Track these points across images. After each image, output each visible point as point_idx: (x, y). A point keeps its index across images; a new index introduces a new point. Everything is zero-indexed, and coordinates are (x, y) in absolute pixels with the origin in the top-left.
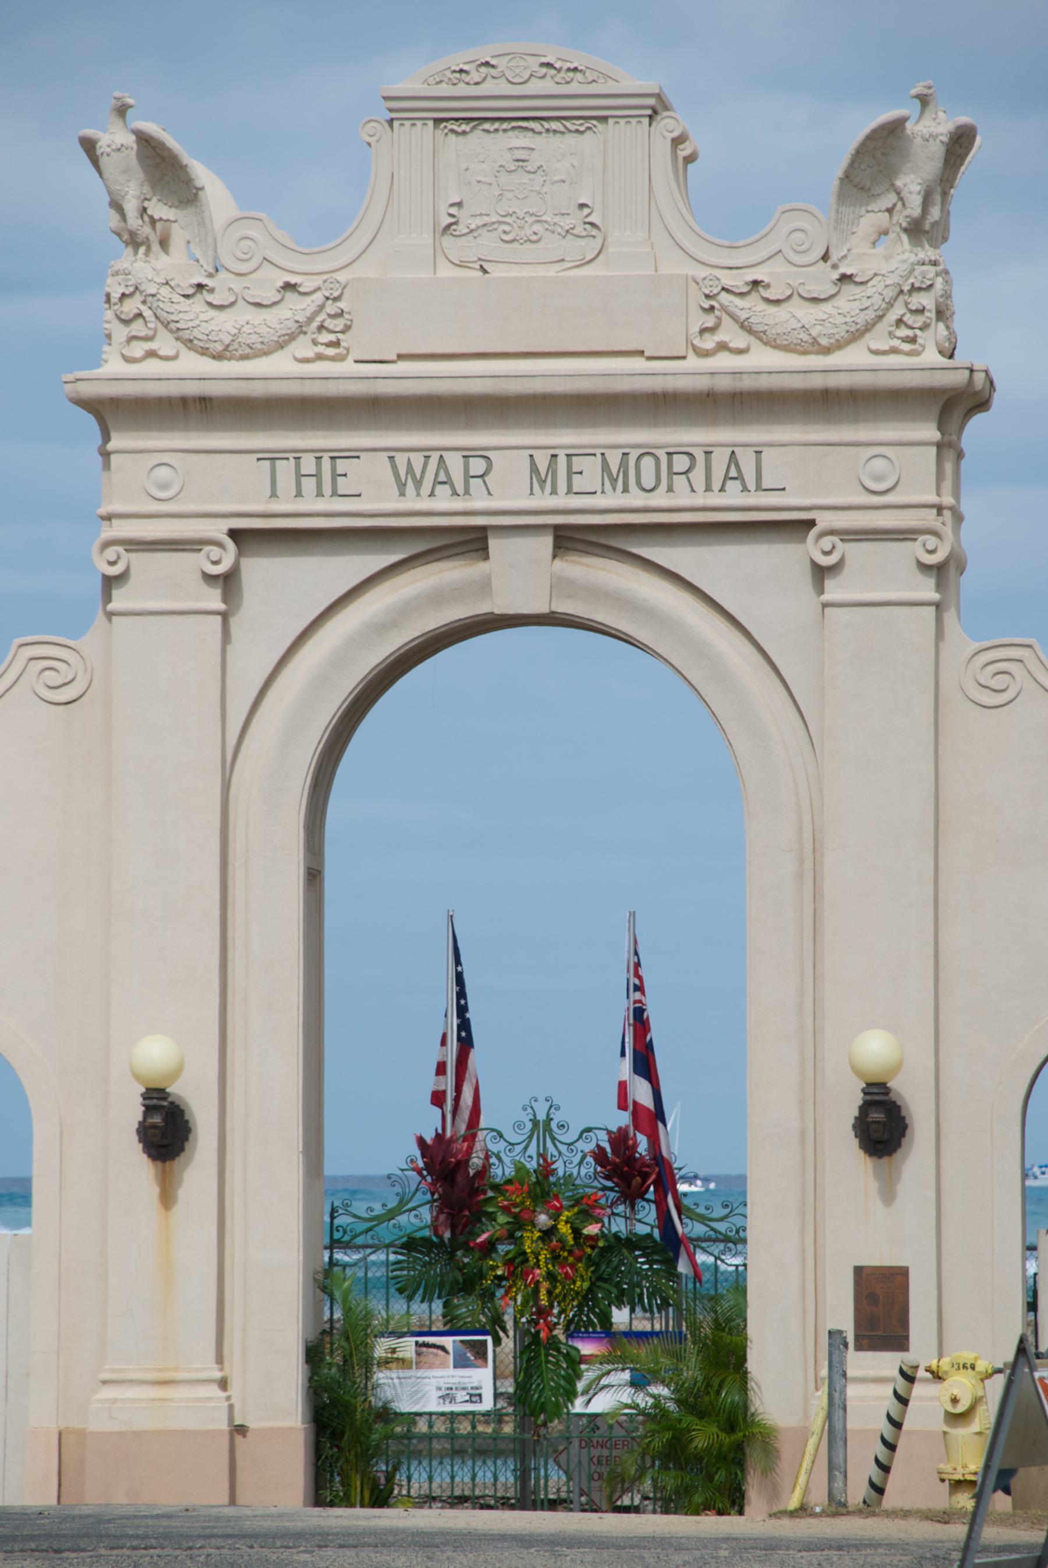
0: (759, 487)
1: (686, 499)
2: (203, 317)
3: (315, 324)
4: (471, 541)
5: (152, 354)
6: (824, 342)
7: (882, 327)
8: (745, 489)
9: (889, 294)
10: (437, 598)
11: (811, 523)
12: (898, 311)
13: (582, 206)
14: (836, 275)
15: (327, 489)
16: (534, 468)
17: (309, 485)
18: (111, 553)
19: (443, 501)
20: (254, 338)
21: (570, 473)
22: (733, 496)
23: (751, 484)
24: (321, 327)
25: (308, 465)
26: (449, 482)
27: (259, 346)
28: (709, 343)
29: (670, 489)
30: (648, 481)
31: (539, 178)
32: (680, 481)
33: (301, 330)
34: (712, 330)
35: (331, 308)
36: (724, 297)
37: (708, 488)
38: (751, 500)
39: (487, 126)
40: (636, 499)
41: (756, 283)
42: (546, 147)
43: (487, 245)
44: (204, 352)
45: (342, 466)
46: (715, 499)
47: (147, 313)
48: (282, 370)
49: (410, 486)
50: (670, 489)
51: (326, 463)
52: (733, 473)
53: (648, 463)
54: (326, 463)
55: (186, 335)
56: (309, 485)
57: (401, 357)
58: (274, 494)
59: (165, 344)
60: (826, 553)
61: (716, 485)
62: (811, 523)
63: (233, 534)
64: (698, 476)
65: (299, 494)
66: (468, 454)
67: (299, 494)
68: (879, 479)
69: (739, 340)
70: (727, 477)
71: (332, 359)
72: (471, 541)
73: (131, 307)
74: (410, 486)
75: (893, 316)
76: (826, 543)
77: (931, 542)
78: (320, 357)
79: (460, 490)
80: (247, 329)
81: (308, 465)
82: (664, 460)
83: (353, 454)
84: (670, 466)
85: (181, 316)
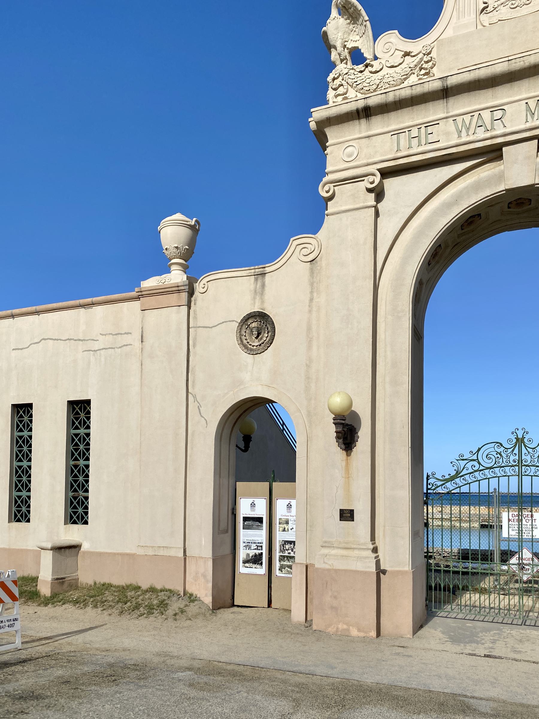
2: (367, 77)
3: (418, 69)
4: (493, 153)
15: (423, 142)
16: (528, 108)
17: (415, 142)
18: (326, 188)
19: (481, 134)
24: (421, 69)
27: (392, 83)
35: (425, 59)
45: (430, 130)
47: (343, 82)
51: (423, 130)
54: (423, 130)
55: (360, 87)
66: (493, 109)
80: (387, 76)
85: (358, 79)
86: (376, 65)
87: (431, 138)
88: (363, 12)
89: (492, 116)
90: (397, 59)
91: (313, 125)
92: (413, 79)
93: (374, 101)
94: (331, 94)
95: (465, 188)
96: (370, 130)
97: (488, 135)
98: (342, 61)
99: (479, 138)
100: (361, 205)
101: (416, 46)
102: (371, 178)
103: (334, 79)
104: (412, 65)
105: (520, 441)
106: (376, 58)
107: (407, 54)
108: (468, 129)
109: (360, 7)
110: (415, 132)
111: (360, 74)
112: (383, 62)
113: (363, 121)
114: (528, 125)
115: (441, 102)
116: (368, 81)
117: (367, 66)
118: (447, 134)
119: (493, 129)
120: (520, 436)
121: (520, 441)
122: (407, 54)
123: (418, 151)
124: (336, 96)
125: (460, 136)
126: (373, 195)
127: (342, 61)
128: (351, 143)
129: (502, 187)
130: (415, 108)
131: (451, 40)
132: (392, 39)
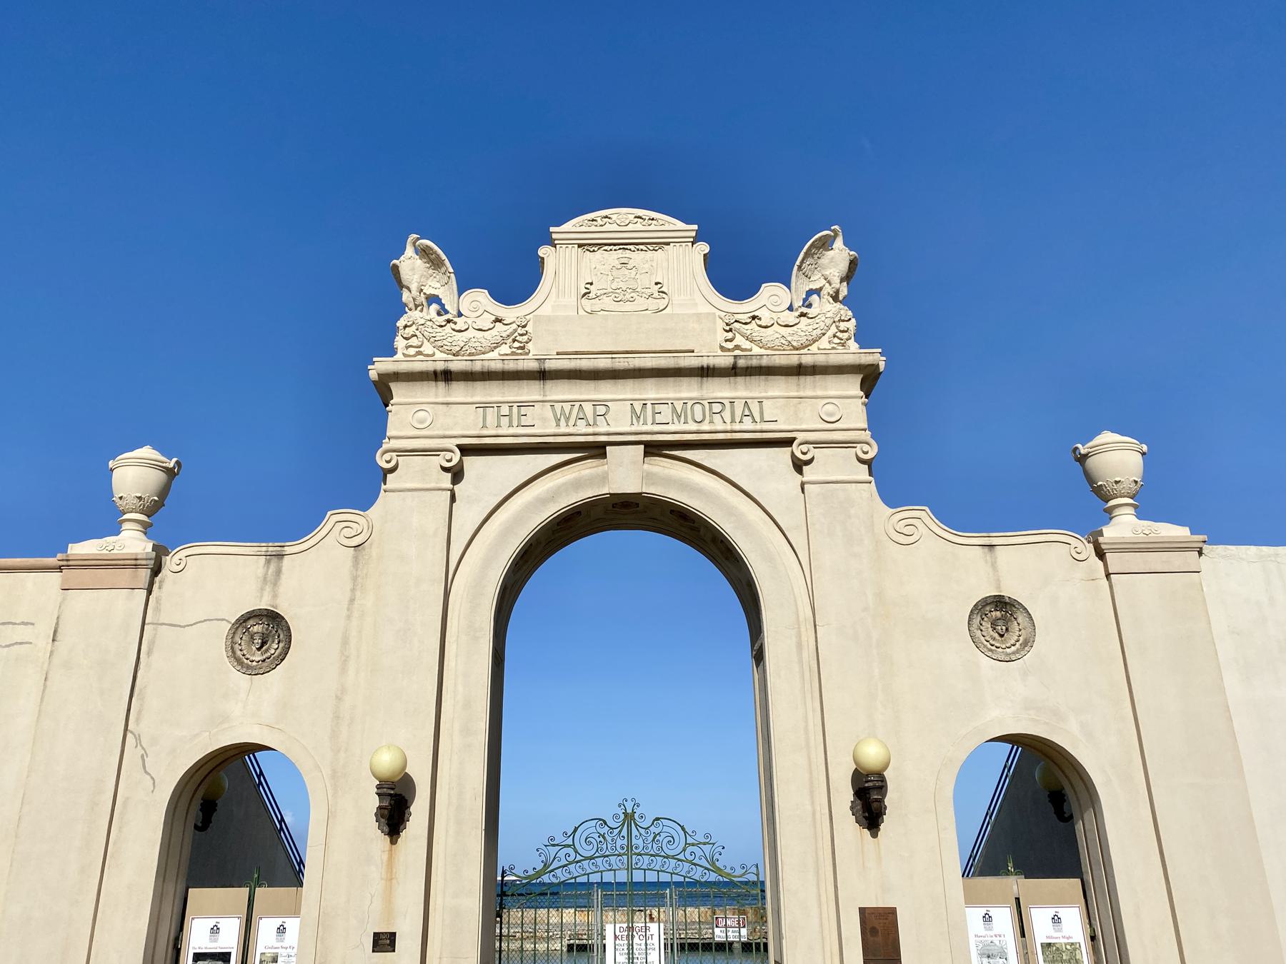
1: (719, 426)
4: (596, 450)
5: (419, 353)
6: (795, 344)
7: (825, 338)
9: (829, 322)
10: (577, 485)
11: (794, 439)
12: (833, 329)
14: (797, 313)
15: (515, 423)
17: (505, 421)
18: (387, 457)
19: (582, 427)
22: (748, 424)
23: (758, 419)
24: (514, 341)
25: (505, 410)
28: (730, 345)
29: (711, 422)
30: (699, 417)
31: (633, 272)
32: (717, 418)
34: (731, 340)
35: (521, 331)
37: (733, 421)
38: (758, 427)
40: (694, 427)
41: (754, 318)
42: (636, 257)
43: (607, 302)
44: (449, 352)
45: (523, 411)
46: (737, 427)
48: (493, 361)
49: (563, 422)
50: (711, 422)
51: (515, 409)
53: (698, 408)
54: (515, 409)
55: (439, 343)
59: (427, 348)
60: (804, 454)
61: (738, 420)
62: (794, 439)
63: (458, 446)
66: (596, 403)
67: (499, 426)
68: (831, 415)
69: (746, 345)
72: (596, 450)
73: (409, 331)
74: (563, 422)
75: (830, 333)
76: (804, 448)
77: (866, 448)
82: (707, 406)
83: (531, 404)
84: (711, 409)
86: (461, 323)
87: (524, 421)
88: (447, 262)
89: (595, 410)
90: (486, 321)
91: (373, 375)
92: (505, 349)
93: (457, 365)
94: (400, 343)
95: (564, 484)
96: (450, 395)
97: (590, 430)
98: (416, 306)
99: (580, 431)
100: (433, 485)
101: (511, 313)
102: (448, 455)
103: (406, 327)
104: (504, 335)
105: (629, 818)
106: (460, 315)
107: (498, 320)
108: (567, 419)
109: (444, 257)
110: (505, 410)
111: (440, 329)
112: (470, 321)
113: (441, 385)
114: (634, 429)
115: (537, 382)
117: (449, 321)
118: (544, 420)
119: (595, 424)
120: (629, 811)
121: (629, 818)
122: (498, 320)
123: (508, 433)
124: (407, 347)
125: (558, 425)
126: (449, 475)
127: (416, 306)
128: (423, 407)
129: (605, 490)
130: (506, 382)
131: (549, 319)
132: (479, 298)
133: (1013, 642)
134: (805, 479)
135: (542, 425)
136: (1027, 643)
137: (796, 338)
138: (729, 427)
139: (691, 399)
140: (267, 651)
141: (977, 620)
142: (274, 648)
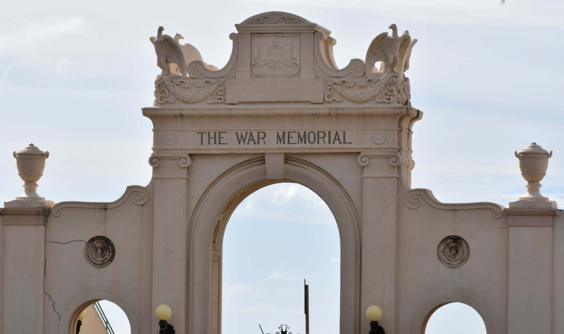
0: (344, 142)
1: (323, 146)
2: (182, 91)
8: (340, 143)
11: (359, 153)
13: (294, 58)
15: (217, 142)
17: (212, 141)
20: (197, 97)
21: (289, 137)
23: (342, 142)
25: (212, 135)
26: (253, 140)
29: (318, 143)
30: (312, 140)
33: (211, 94)
36: (335, 86)
37: (329, 142)
39: (266, 35)
41: (344, 82)
44: (182, 101)
49: (242, 141)
50: (318, 143)
52: (337, 138)
53: (312, 135)
55: (177, 96)
56: (212, 141)
57: (240, 103)
58: (202, 143)
62: (359, 153)
64: (326, 139)
65: (209, 143)
67: (209, 143)
70: (335, 139)
71: (219, 103)
74: (242, 141)
76: (364, 159)
78: (216, 103)
79: (256, 142)
80: (195, 95)
81: (212, 135)
99: (251, 147)
108: (244, 141)
116: (182, 94)
119: (258, 143)
123: (214, 148)
125: (239, 143)
133: (458, 258)
134: (364, 176)
135: (231, 143)
136: (464, 260)
137: (364, 96)
138: (327, 145)
139: (308, 130)
140: (104, 256)
141: (442, 247)
142: (108, 255)
